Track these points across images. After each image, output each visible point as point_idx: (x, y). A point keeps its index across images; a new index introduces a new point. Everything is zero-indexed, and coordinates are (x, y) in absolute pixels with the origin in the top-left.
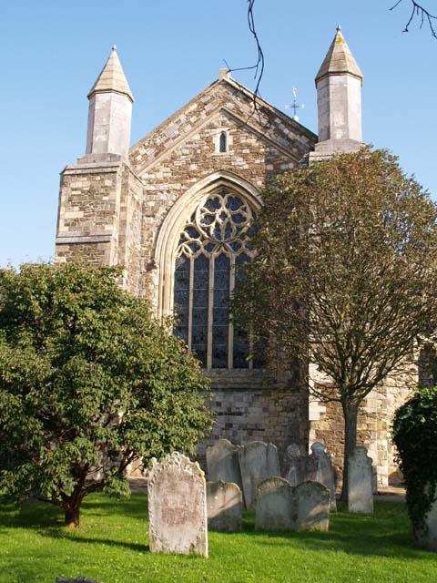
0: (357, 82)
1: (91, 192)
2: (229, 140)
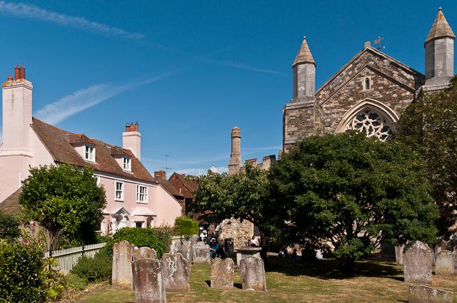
0: (452, 41)
2: (371, 83)
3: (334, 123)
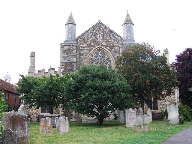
1: (69, 50)
3: (85, 54)
